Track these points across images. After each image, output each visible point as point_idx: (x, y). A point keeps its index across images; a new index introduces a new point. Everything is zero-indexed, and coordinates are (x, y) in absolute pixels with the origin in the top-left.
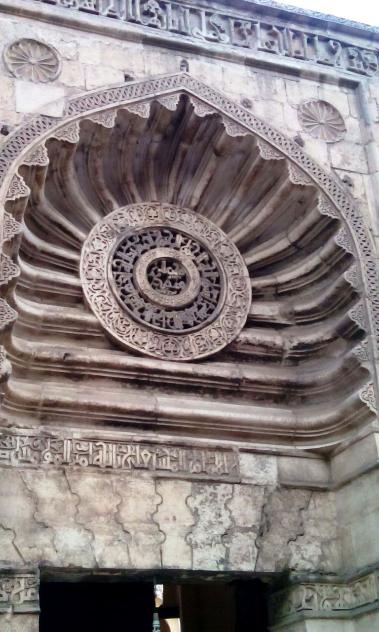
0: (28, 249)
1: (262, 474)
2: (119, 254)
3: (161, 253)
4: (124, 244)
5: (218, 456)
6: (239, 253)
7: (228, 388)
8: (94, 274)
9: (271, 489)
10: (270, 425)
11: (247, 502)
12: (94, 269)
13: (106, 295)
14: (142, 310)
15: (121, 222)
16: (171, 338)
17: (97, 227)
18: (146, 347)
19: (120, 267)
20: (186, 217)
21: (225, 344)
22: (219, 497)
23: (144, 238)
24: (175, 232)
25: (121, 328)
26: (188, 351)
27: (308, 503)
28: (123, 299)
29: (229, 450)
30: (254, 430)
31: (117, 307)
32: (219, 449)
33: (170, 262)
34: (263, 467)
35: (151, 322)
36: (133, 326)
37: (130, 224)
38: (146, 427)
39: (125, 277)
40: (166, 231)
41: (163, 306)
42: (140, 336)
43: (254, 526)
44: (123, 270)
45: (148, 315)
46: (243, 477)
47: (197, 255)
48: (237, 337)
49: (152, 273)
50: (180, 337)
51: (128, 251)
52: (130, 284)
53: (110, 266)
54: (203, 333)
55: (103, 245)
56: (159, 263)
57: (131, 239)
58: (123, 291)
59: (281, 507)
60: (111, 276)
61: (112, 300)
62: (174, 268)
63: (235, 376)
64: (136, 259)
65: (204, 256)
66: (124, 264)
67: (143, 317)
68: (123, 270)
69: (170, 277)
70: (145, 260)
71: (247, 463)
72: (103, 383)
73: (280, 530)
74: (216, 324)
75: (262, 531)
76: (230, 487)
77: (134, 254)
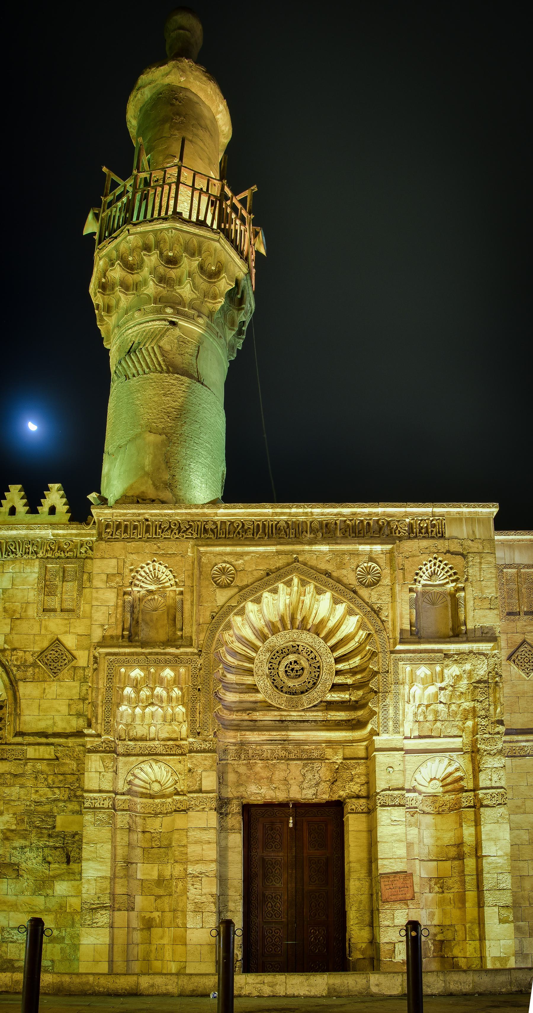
2: (272, 661)
3: (292, 658)
4: (274, 655)
6: (330, 651)
8: (260, 673)
11: (328, 770)
12: (260, 671)
14: (282, 688)
15: (271, 644)
17: (261, 649)
19: (272, 668)
20: (304, 636)
22: (315, 768)
23: (284, 650)
24: (298, 646)
25: (272, 698)
27: (356, 768)
28: (273, 683)
31: (270, 687)
33: (295, 662)
34: (336, 754)
37: (277, 644)
40: (294, 645)
44: (273, 669)
47: (309, 655)
49: (287, 669)
51: (276, 658)
53: (267, 668)
55: (264, 657)
56: (291, 663)
57: (277, 652)
60: (268, 673)
61: (268, 684)
62: (297, 664)
64: (280, 662)
65: (312, 655)
66: (274, 666)
68: (273, 669)
69: (295, 669)
70: (285, 662)
71: (329, 752)
74: (316, 690)
76: (320, 764)
77: (278, 659)
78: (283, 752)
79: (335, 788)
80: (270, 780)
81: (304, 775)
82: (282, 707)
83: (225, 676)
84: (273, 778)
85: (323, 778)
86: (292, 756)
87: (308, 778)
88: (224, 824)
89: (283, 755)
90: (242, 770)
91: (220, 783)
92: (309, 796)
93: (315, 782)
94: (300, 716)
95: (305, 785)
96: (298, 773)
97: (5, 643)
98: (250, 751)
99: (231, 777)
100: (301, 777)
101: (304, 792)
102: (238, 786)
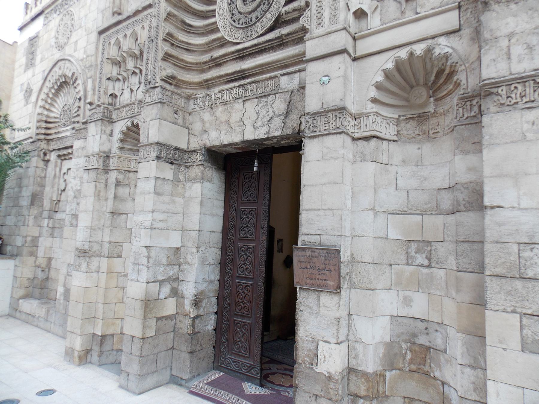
0: (202, 13)
1: (291, 84)
5: (270, 82)
7: (278, 44)
8: (221, 12)
9: (295, 91)
10: (293, 57)
13: (225, 20)
16: (250, 28)
18: (239, 39)
21: (274, 19)
22: (269, 102)
26: (257, 32)
28: (232, 18)
29: (276, 77)
30: (288, 62)
31: (229, 24)
32: (271, 78)
35: (242, 25)
36: (235, 30)
38: (244, 78)
39: (233, 6)
41: (247, 13)
42: (237, 35)
43: (283, 113)
45: (241, 22)
46: (281, 89)
48: (280, 12)
50: (253, 26)
52: (236, 9)
54: (264, 19)
58: (233, 14)
59: (298, 99)
63: (277, 36)
67: (239, 24)
72: (229, 63)
73: (297, 112)
74: (270, 10)
75: (287, 115)
76: (274, 96)
78: (241, 90)
79: (288, 121)
80: (228, 122)
81: (258, 113)
82: (238, 41)
83: (190, 26)
84: (230, 121)
85: (277, 113)
86: (248, 93)
87: (261, 116)
88: (190, 174)
89: (240, 94)
90: (207, 116)
91: (189, 134)
92: (262, 136)
93: (269, 119)
94: (255, 45)
95: (259, 123)
96: (253, 111)
97: (84, 54)
98: (213, 98)
99: (197, 127)
100: (255, 115)
101: (257, 132)
102: (202, 134)
